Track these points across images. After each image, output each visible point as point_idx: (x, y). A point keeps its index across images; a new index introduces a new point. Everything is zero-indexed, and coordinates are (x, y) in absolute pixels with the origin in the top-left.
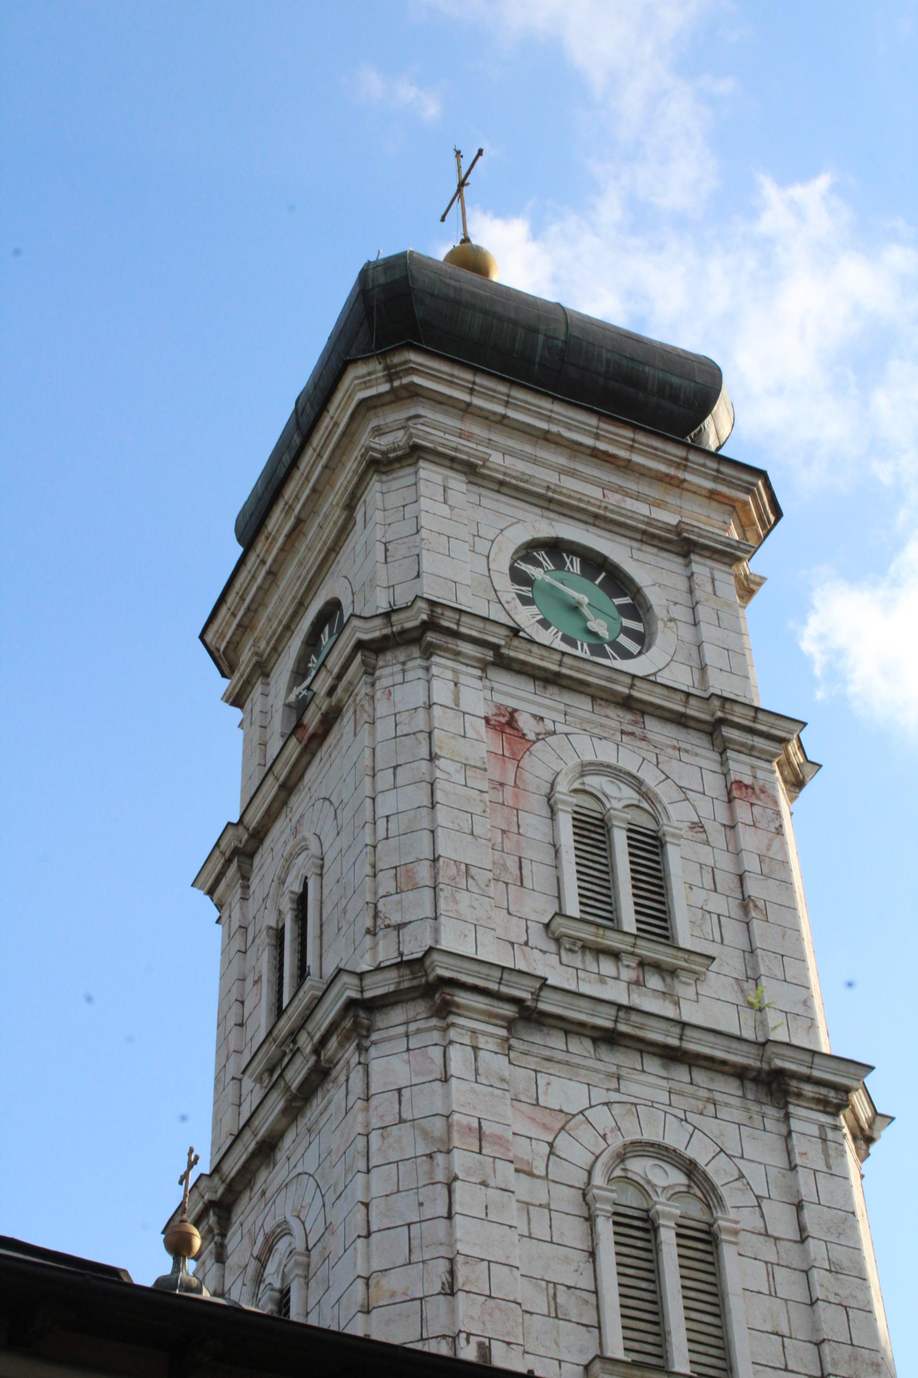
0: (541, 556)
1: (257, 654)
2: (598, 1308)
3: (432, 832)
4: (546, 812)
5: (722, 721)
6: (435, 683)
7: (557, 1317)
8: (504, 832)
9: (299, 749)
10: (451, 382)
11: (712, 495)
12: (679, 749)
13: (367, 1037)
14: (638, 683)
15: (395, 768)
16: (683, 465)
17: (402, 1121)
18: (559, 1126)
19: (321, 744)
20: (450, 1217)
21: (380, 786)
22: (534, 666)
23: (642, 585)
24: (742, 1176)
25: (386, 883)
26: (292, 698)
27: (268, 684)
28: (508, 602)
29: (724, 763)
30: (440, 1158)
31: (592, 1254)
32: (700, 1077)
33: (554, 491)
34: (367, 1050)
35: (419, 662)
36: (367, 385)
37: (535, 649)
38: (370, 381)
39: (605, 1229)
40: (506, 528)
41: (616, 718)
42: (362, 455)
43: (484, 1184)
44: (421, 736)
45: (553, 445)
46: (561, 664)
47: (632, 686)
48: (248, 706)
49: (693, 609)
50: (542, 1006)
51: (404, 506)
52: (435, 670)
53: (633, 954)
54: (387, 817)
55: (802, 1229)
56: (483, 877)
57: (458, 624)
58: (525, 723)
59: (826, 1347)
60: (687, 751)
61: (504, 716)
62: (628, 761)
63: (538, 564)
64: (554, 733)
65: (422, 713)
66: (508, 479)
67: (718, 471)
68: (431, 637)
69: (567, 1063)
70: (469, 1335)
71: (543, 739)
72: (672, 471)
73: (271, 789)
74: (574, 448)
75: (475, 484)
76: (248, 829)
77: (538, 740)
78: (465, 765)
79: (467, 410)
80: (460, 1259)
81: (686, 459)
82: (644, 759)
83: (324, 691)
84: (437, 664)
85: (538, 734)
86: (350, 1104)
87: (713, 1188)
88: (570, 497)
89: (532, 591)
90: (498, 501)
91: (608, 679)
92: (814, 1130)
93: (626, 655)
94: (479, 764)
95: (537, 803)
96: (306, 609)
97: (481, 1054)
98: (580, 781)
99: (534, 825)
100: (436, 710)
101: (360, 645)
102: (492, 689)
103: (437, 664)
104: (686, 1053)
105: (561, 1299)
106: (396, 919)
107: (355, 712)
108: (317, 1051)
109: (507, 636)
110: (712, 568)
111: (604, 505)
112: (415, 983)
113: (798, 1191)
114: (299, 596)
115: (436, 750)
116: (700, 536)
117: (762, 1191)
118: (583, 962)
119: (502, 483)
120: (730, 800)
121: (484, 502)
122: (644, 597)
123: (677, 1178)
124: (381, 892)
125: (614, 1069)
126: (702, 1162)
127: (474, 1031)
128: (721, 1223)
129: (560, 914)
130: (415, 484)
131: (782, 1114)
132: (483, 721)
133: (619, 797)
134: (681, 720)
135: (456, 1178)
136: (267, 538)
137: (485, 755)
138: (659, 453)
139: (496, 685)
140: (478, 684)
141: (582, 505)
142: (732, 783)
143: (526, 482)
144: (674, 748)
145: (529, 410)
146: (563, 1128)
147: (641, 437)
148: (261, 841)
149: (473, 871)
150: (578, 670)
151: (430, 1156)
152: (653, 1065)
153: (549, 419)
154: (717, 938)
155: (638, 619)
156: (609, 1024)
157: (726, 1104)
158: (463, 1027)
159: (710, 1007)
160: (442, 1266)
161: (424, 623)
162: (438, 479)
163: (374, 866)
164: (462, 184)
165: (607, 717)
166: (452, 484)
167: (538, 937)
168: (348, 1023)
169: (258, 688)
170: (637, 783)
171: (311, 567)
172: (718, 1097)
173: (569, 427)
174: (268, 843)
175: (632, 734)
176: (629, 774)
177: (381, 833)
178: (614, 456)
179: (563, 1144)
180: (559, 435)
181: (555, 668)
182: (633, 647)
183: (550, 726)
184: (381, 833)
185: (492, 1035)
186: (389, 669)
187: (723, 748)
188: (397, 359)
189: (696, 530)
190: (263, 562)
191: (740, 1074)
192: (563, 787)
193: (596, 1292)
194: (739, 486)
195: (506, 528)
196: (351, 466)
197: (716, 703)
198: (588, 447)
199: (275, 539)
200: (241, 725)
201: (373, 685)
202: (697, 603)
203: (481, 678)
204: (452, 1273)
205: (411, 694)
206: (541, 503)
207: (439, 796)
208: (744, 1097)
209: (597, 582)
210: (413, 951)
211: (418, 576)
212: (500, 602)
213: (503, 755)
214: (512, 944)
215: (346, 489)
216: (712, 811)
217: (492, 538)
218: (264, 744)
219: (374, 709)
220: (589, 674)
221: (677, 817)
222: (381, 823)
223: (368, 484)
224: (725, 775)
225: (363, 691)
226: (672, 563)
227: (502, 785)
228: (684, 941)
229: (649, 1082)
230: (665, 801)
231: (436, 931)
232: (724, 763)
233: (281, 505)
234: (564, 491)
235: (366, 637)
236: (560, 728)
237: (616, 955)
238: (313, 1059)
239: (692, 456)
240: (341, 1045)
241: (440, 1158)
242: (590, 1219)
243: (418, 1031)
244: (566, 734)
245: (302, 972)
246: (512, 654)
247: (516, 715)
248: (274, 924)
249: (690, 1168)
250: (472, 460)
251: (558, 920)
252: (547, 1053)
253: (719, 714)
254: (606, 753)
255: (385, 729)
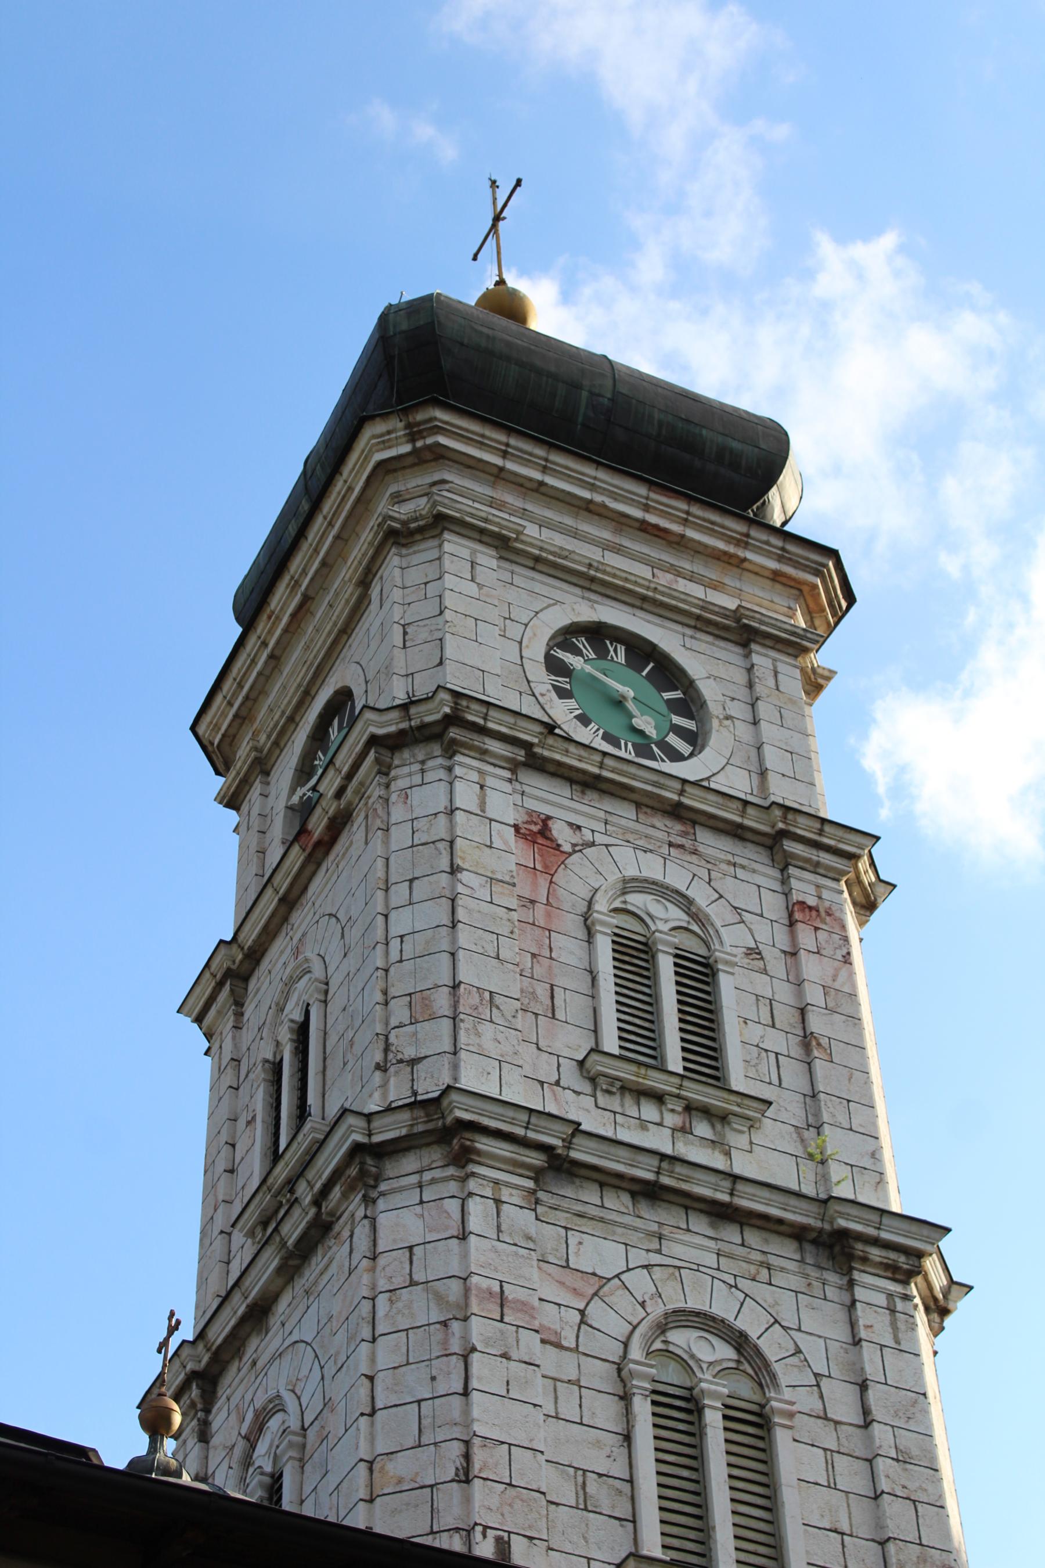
0: (581, 642)
1: (255, 749)
2: (633, 1499)
3: (453, 954)
4: (582, 934)
5: (784, 834)
6: (459, 785)
7: (586, 1509)
8: (534, 955)
9: (302, 858)
10: (482, 443)
11: (776, 577)
12: (735, 865)
13: (375, 1187)
14: (689, 789)
15: (411, 881)
16: (743, 542)
17: (413, 1283)
18: (591, 1291)
19: (327, 853)
20: (466, 1393)
21: (394, 902)
22: (571, 768)
23: (695, 677)
24: (798, 1351)
25: (399, 1012)
26: (295, 799)
27: (268, 784)
28: (542, 695)
29: (785, 881)
30: (455, 1326)
31: (627, 1438)
32: (753, 1238)
33: (597, 570)
34: (374, 1201)
35: (440, 761)
36: (385, 445)
37: (572, 748)
38: (389, 440)
39: (643, 1409)
40: (541, 610)
41: (663, 828)
42: (379, 525)
43: (505, 1356)
44: (441, 845)
45: (596, 517)
46: (601, 766)
47: (682, 793)
48: (245, 807)
49: (753, 705)
50: (574, 1154)
51: (426, 584)
52: (458, 771)
53: (678, 1096)
54: (402, 937)
55: (866, 1411)
56: (509, 1006)
57: (485, 719)
58: (561, 833)
59: (891, 1547)
60: (743, 867)
61: (536, 824)
62: (677, 878)
63: (578, 652)
64: (593, 844)
65: (442, 819)
66: (544, 555)
67: (783, 549)
68: (454, 733)
69: (602, 1220)
70: (486, 1528)
71: (580, 851)
72: (732, 549)
73: (270, 903)
74: (621, 521)
75: (507, 560)
76: (242, 949)
77: (575, 852)
78: (491, 879)
79: (499, 475)
80: (477, 1441)
81: (747, 535)
82: (694, 875)
83: (331, 793)
84: (460, 764)
85: (574, 845)
86: (354, 1263)
87: (767, 1364)
88: (614, 576)
89: (570, 683)
90: (533, 579)
91: (655, 784)
92: (882, 1300)
93: (676, 756)
94: (507, 879)
95: (572, 923)
96: (313, 698)
97: (505, 1207)
98: (622, 899)
99: (568, 948)
100: (459, 816)
101: (374, 741)
102: (523, 793)
103: (460, 764)
104: (737, 1210)
105: (592, 1488)
106: (409, 1053)
107: (367, 817)
108: (317, 1202)
109: (541, 733)
110: (774, 660)
111: (653, 585)
112: (430, 1126)
113: (862, 1369)
114: (305, 683)
115: (458, 861)
116: (761, 622)
117: (821, 1368)
118: (622, 1106)
119: (537, 559)
120: (792, 924)
121: (517, 580)
122: (697, 691)
123: (725, 1352)
124: (393, 1022)
125: (655, 1227)
126: (753, 1334)
127: (496, 1183)
128: (774, 1404)
129: (596, 1050)
130: (439, 559)
131: (846, 1279)
132: (512, 829)
133: (666, 917)
134: (736, 832)
135: (474, 1349)
136: (269, 617)
137: (514, 868)
138: (716, 528)
139: (527, 789)
140: (507, 787)
142: (794, 904)
143: (565, 558)
144: (729, 863)
145: (569, 476)
146: (596, 1294)
147: (696, 510)
148: (258, 962)
149: (498, 1000)
151: (445, 1324)
152: (699, 1224)
153: (592, 488)
154: (775, 1080)
155: (691, 717)
156: (650, 1176)
157: (782, 1269)
158: (484, 1177)
159: (764, 1156)
160: (456, 1449)
161: (446, 716)
162: (465, 553)
163: (385, 993)
164: (497, 218)
165: (654, 827)
166: (481, 559)
167: (570, 1076)
168: (353, 1171)
169: (257, 788)
170: (685, 903)
171: (319, 651)
172: (773, 1260)
173: (615, 497)
174: (265, 964)
175: (681, 846)
176: (678, 892)
177: (394, 955)
178: (666, 531)
179: (595, 1310)
180: (604, 506)
181: (596, 770)
182: (684, 748)
183: (588, 836)
184: (394, 955)
185: (517, 1187)
186: (406, 770)
187: (784, 864)
188: (420, 417)
189: (758, 616)
190: (265, 644)
191: (799, 1234)
192: (601, 905)
193: (631, 1481)
195: (541, 610)
196: (366, 537)
197: (777, 813)
198: (637, 520)
199: (278, 619)
200: (236, 830)
201: (387, 786)
202: (757, 699)
203: (510, 781)
204: (467, 1456)
205: (430, 797)
206: (581, 582)
207: (461, 914)
208: (802, 1261)
209: (644, 673)
210: (428, 1088)
211: (441, 663)
212: (534, 695)
213: (534, 868)
214: (542, 1083)
215: (360, 563)
216: (770, 935)
217: (526, 622)
218: (262, 852)
219: (388, 814)
220: (634, 777)
221: (731, 941)
222: (395, 944)
223: (385, 558)
224: (787, 895)
225: (376, 793)
226: (730, 653)
227: (533, 902)
228: (737, 1081)
229: (694, 1243)
230: (718, 924)
231: (455, 1067)
232: (785, 881)
233: (286, 579)
234: (608, 569)
235: (380, 732)
236: (599, 838)
237: (659, 1098)
238: (313, 1211)
239: (754, 533)
240: (345, 1196)
241: (455, 1326)
242: (626, 1398)
243: (433, 1181)
244: (607, 846)
245: (302, 1112)
246: (546, 753)
247: (550, 823)
248: (270, 1057)
249: (740, 1341)
250: (504, 532)
251: (595, 1057)
252: (579, 1208)
253: (781, 825)
254: (652, 868)
255: (400, 836)
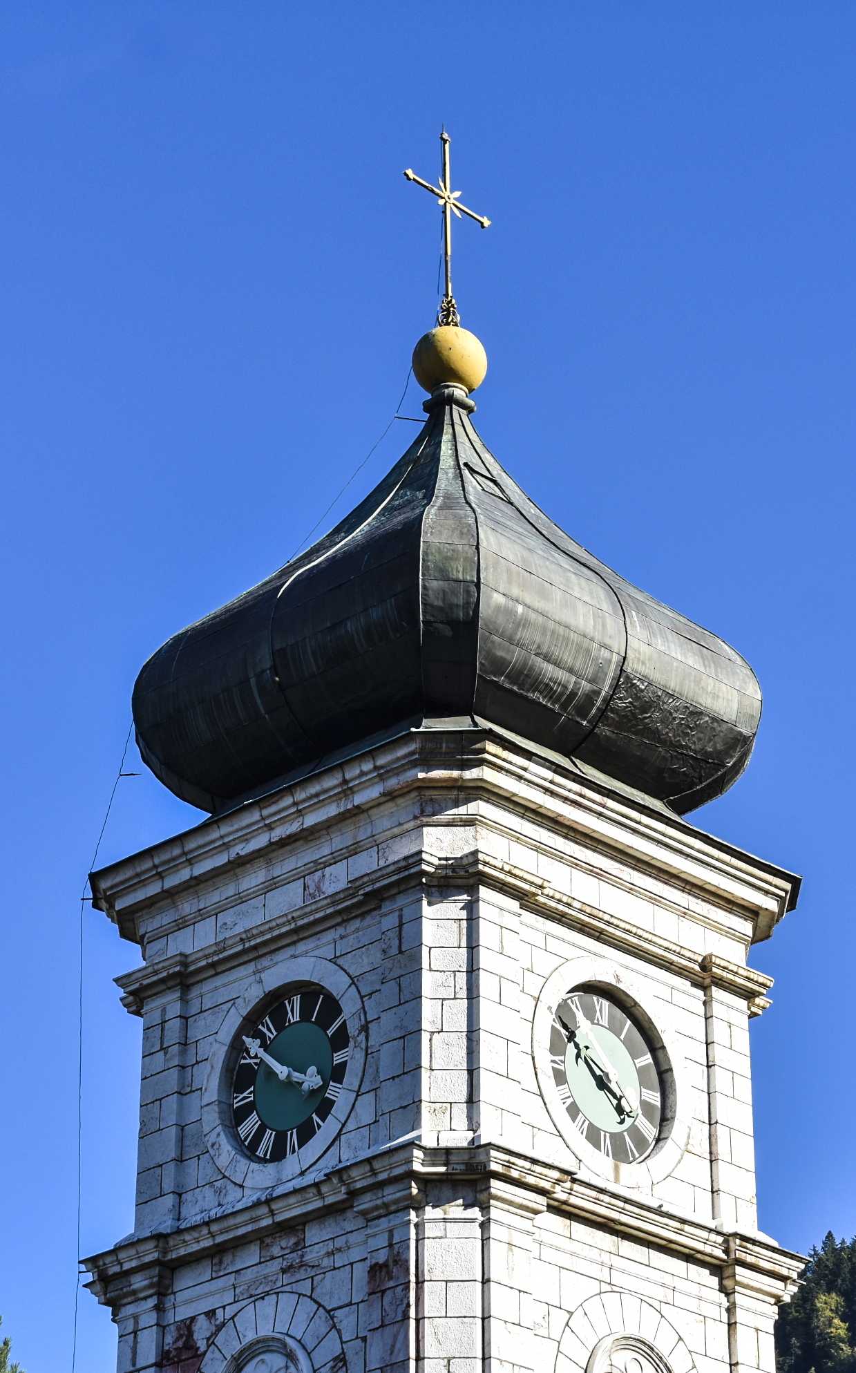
11: (390, 796)
67: (376, 768)
81: (345, 782)
88: (262, 933)
116: (373, 882)
141: (276, 933)
143: (224, 949)
147: (300, 795)
150: (227, 1230)
173: (245, 839)
189: (365, 879)
194: (403, 765)
206: (251, 956)
234: (255, 932)
250: (171, 971)
